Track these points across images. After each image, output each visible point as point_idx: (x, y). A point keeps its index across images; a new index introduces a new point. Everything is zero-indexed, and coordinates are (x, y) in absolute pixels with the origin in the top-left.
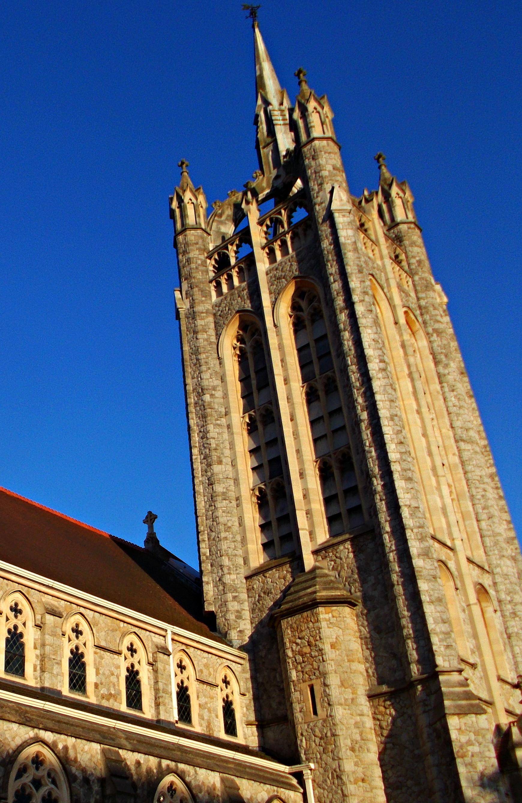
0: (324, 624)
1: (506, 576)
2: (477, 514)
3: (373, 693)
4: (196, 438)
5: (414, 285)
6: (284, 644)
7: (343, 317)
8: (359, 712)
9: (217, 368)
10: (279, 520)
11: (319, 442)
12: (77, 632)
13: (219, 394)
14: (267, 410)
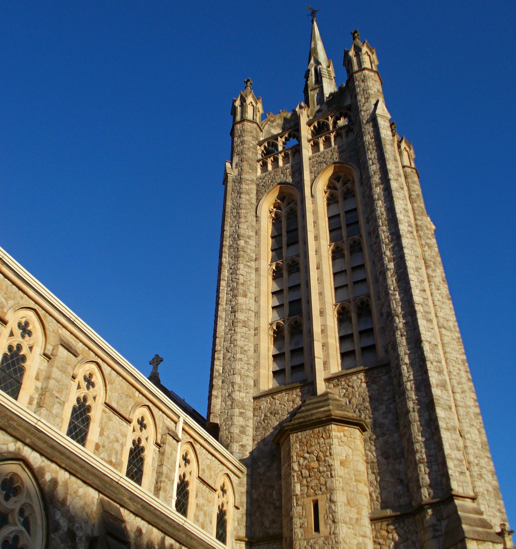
0: (335, 441)
1: (474, 442)
2: (453, 387)
3: (376, 516)
4: (225, 273)
5: (413, 210)
6: (289, 457)
7: (378, 191)
8: (362, 533)
9: (254, 223)
10: (292, 352)
11: (339, 291)
12: (89, 382)
13: (252, 242)
14: (294, 262)
